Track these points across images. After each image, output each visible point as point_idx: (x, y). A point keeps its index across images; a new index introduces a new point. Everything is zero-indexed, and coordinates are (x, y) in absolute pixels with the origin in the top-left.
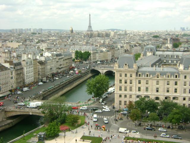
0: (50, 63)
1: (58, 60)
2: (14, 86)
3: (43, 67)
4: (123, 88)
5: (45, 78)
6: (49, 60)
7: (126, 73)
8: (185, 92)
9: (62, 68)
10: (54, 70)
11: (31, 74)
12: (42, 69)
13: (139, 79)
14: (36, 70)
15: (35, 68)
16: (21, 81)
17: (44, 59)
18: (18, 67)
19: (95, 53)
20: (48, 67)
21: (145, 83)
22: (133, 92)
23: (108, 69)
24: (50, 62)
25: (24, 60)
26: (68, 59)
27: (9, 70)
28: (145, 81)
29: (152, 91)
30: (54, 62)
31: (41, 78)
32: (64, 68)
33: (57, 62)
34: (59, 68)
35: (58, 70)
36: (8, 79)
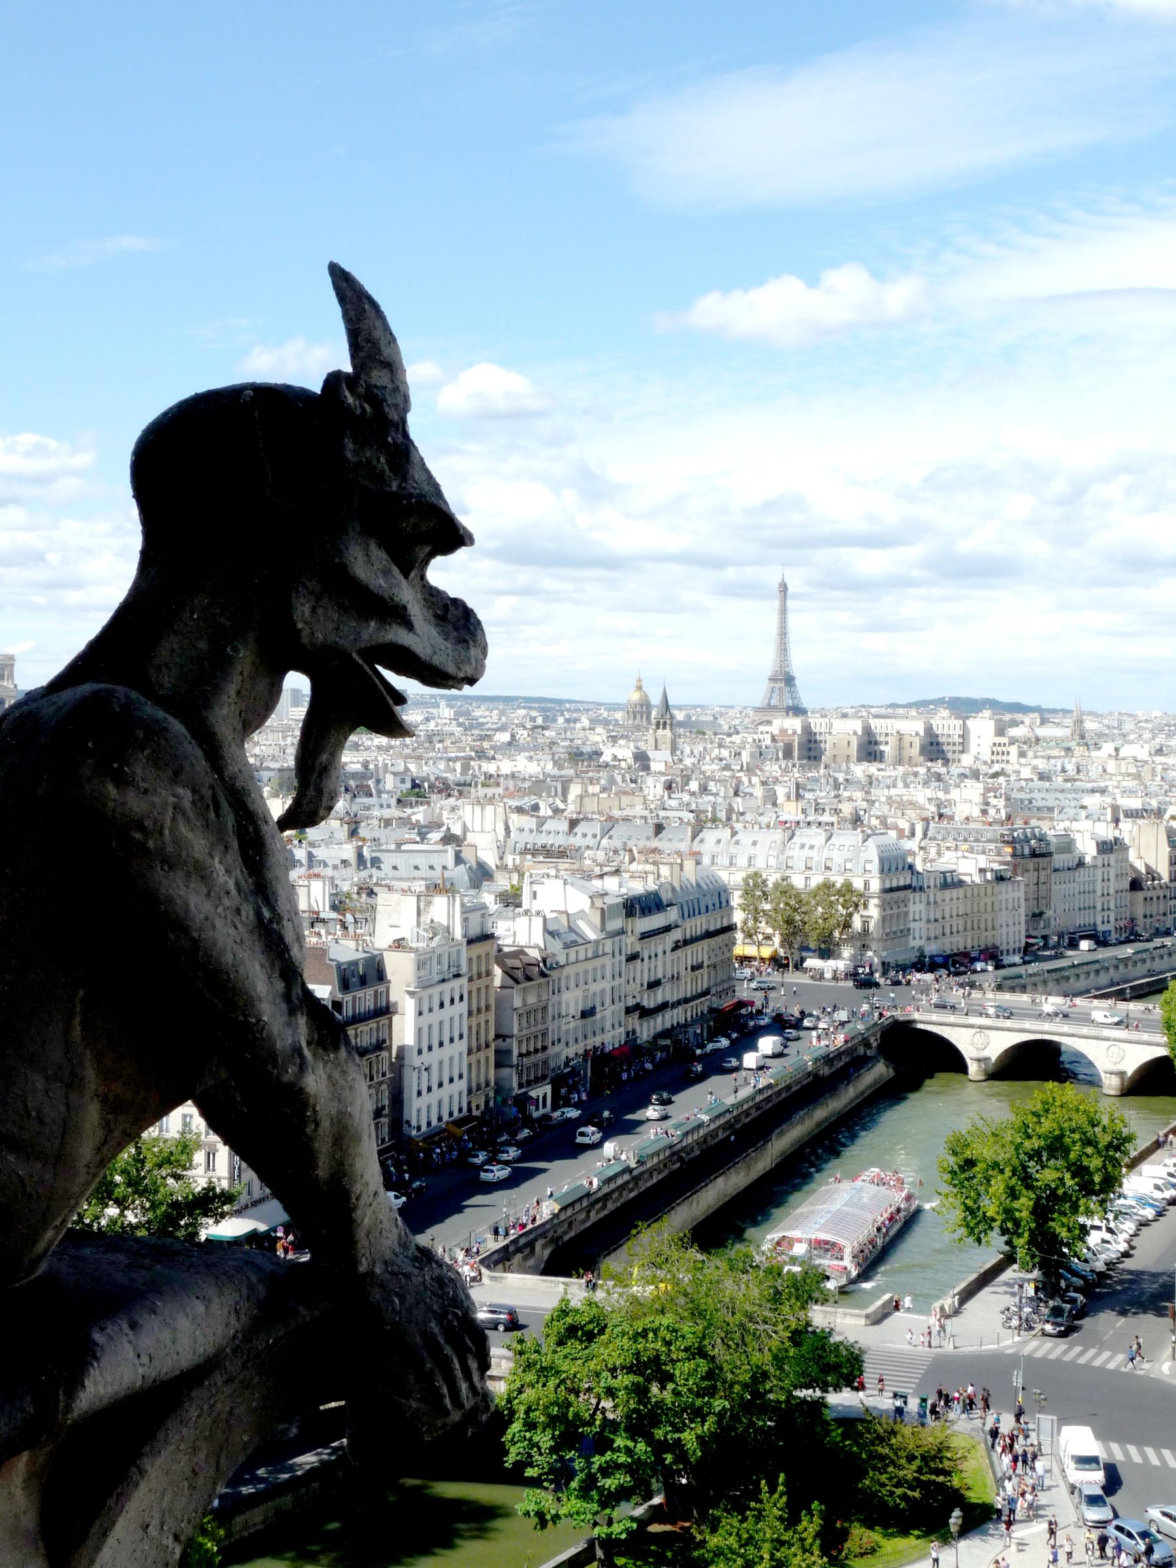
0: (580, 968)
1: (638, 948)
3: (532, 1000)
5: (548, 1089)
9: (664, 1006)
10: (608, 1027)
12: (528, 1014)
14: (487, 1022)
15: (479, 1011)
17: (538, 938)
19: (898, 889)
20: (566, 996)
23: (1027, 1025)
24: (582, 956)
25: (399, 945)
30: (608, 961)
31: (515, 1084)
32: (675, 1005)
35: (634, 1022)
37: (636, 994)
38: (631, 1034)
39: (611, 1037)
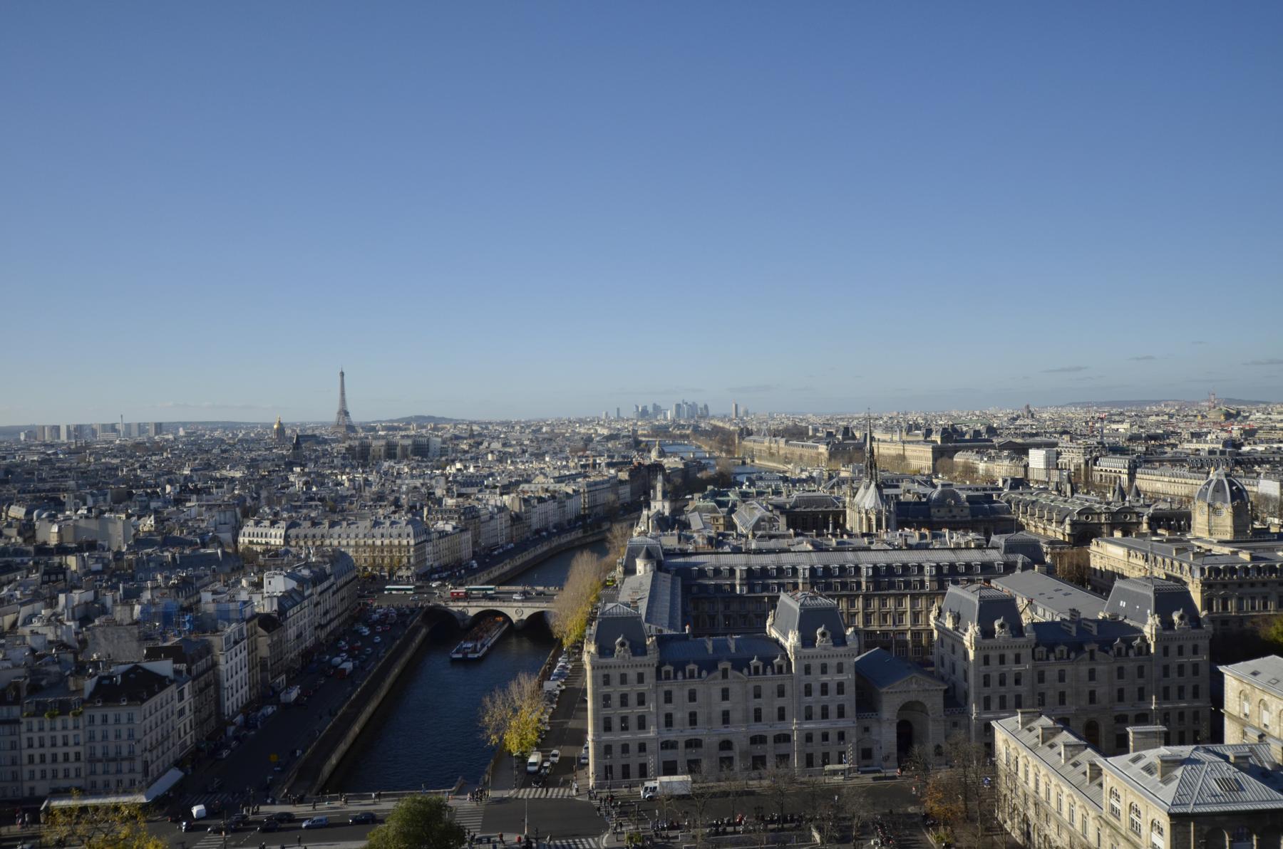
2: (189, 743)
3: (275, 638)
4: (616, 723)
6: (291, 607)
7: (623, 671)
8: (809, 717)
9: (331, 620)
11: (240, 674)
13: (666, 688)
16: (210, 715)
17: (275, 607)
18: (202, 664)
21: (686, 699)
22: (652, 732)
26: (347, 583)
27: (174, 687)
28: (686, 693)
29: (709, 720)
33: (318, 604)
34: (321, 627)
35: (319, 632)
36: (169, 721)
37: (318, 620)
38: (317, 639)
39: (309, 642)
